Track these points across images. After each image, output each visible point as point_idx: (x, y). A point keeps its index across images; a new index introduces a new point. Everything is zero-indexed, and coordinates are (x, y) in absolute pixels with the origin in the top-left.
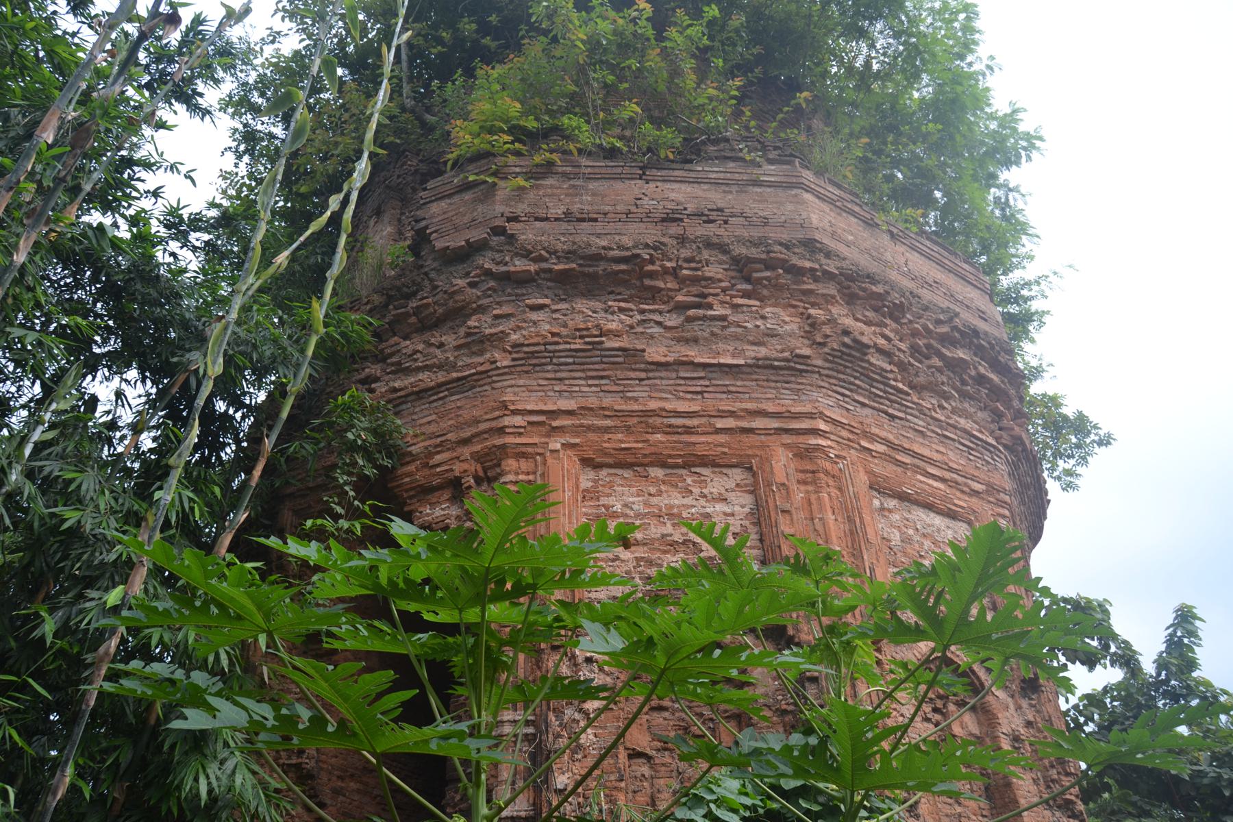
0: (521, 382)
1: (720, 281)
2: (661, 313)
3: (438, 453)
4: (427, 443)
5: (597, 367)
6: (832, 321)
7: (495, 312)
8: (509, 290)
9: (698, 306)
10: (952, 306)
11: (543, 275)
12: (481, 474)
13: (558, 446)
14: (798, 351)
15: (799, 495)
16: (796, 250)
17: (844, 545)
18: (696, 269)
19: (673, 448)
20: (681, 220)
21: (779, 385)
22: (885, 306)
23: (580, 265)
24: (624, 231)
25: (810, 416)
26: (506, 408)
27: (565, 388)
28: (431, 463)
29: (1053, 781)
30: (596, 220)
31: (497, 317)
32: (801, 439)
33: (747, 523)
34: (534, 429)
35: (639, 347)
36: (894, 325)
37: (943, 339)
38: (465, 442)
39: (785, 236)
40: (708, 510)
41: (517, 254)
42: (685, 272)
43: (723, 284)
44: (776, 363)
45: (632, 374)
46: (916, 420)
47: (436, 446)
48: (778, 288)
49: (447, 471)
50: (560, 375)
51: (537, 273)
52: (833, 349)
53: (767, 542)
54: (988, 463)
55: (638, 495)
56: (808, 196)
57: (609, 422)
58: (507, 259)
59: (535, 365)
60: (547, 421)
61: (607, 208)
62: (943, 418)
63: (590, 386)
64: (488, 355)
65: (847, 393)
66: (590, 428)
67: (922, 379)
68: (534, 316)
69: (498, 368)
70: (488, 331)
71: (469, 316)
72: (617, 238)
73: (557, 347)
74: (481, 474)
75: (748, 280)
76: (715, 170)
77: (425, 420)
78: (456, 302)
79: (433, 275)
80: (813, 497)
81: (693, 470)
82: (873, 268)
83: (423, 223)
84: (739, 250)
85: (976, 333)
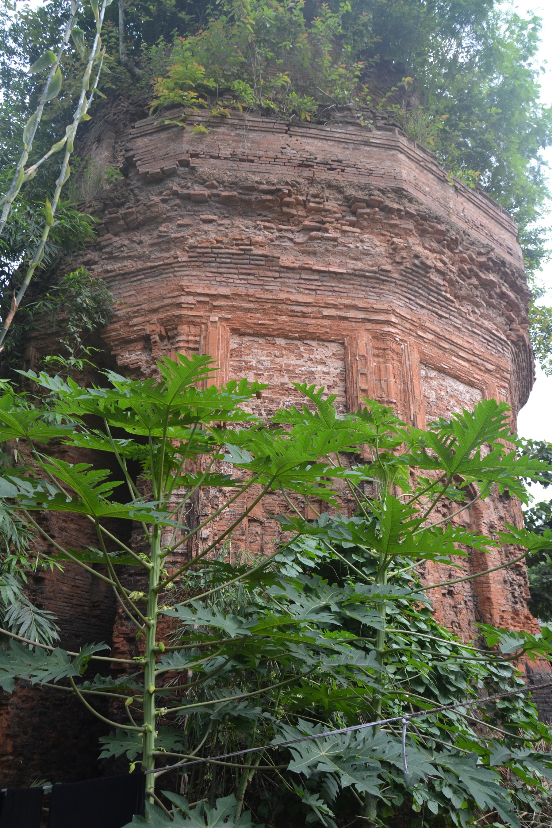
0: (194, 273)
1: (335, 212)
2: (292, 232)
3: (136, 317)
4: (128, 310)
5: (246, 266)
6: (408, 248)
7: (179, 222)
8: (189, 207)
9: (318, 229)
10: (490, 243)
11: (213, 198)
12: (164, 333)
13: (217, 319)
14: (383, 267)
15: (373, 364)
16: (389, 195)
17: (399, 399)
18: (319, 203)
19: (293, 326)
20: (312, 166)
21: (368, 289)
22: (445, 240)
23: (240, 193)
24: (272, 171)
25: (387, 312)
26: (183, 290)
27: (224, 279)
28: (131, 323)
29: (510, 553)
30: (252, 161)
31: (180, 226)
32: (378, 327)
33: (337, 380)
34: (201, 306)
35: (276, 255)
36: (450, 254)
37: (483, 266)
38: (154, 311)
39: (382, 185)
40: (313, 369)
41: (196, 182)
42: (312, 204)
43: (337, 215)
44: (367, 274)
45: (270, 274)
46: (456, 320)
47: (135, 312)
48: (374, 221)
49: (141, 330)
50: (220, 270)
51: (209, 196)
52: (407, 268)
53: (349, 393)
54: (499, 351)
55: (268, 356)
56: (401, 156)
57: (251, 305)
58: (189, 184)
59: (204, 262)
60: (210, 301)
61: (261, 153)
62: (474, 320)
63: (241, 279)
64: (172, 253)
65: (413, 298)
66: (238, 308)
67: (463, 292)
68: (206, 227)
69: (179, 262)
70: (173, 235)
71: (161, 223)
72: (267, 175)
73: (220, 251)
74: (164, 333)
75: (354, 213)
76: (339, 132)
77: (127, 294)
78: (152, 212)
79: (136, 191)
80: (382, 366)
81: (305, 342)
82: (441, 212)
83: (131, 153)
84: (351, 192)
85: (503, 263)
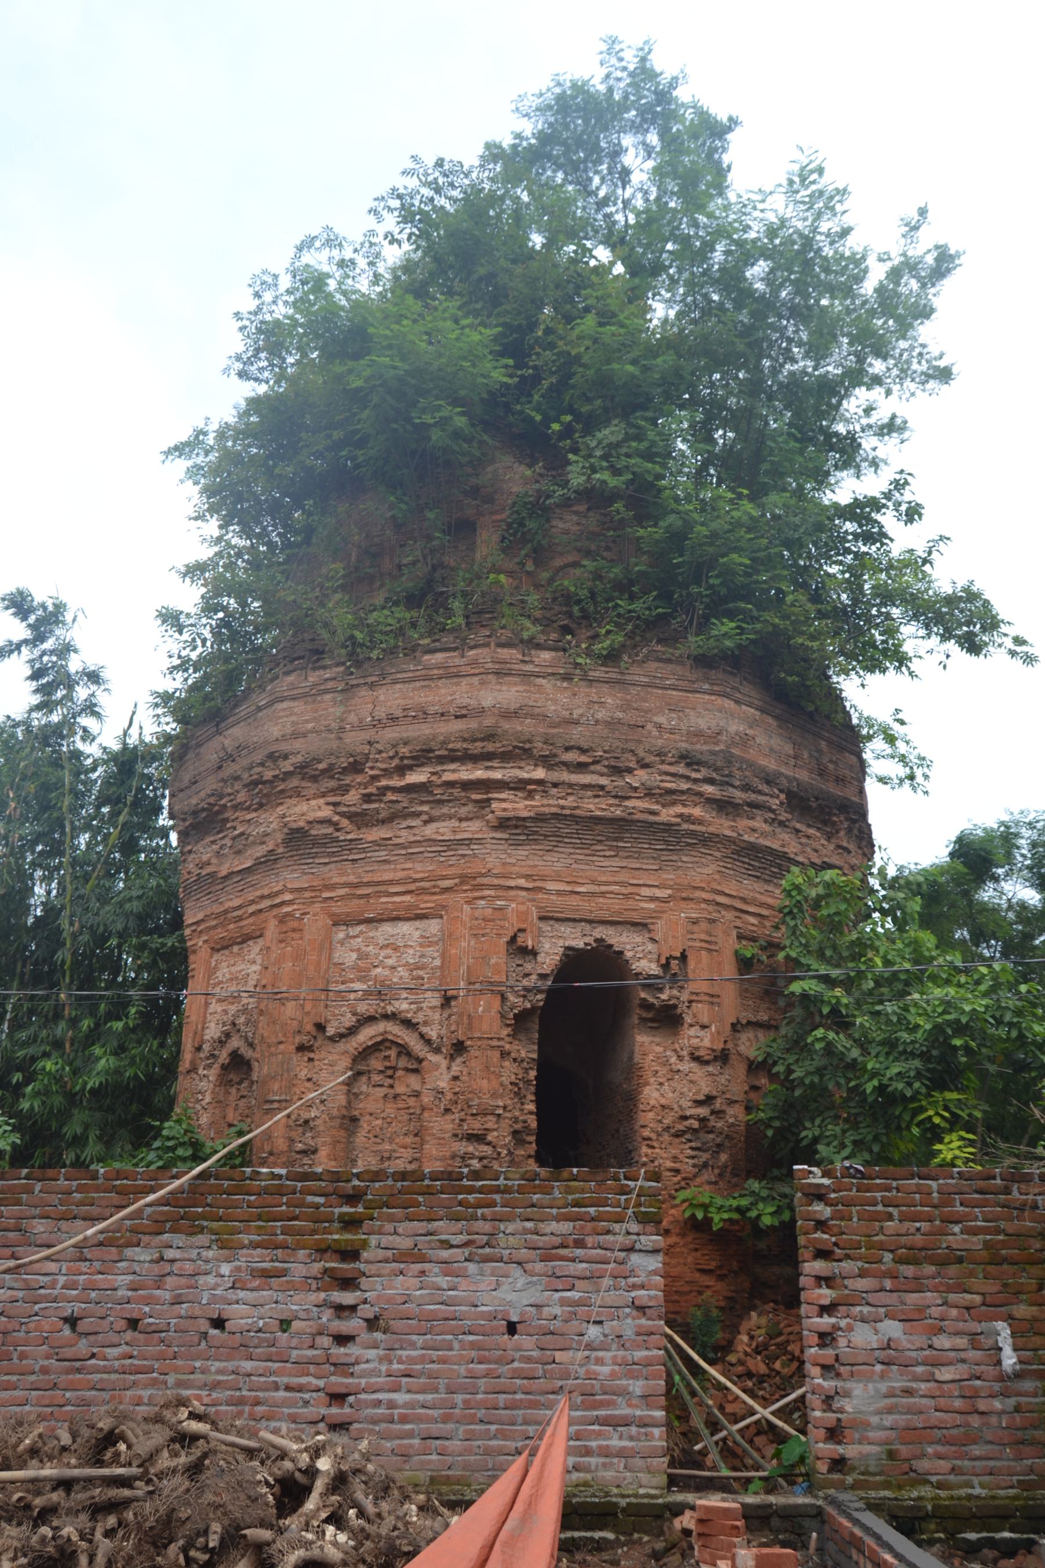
67: (383, 815)
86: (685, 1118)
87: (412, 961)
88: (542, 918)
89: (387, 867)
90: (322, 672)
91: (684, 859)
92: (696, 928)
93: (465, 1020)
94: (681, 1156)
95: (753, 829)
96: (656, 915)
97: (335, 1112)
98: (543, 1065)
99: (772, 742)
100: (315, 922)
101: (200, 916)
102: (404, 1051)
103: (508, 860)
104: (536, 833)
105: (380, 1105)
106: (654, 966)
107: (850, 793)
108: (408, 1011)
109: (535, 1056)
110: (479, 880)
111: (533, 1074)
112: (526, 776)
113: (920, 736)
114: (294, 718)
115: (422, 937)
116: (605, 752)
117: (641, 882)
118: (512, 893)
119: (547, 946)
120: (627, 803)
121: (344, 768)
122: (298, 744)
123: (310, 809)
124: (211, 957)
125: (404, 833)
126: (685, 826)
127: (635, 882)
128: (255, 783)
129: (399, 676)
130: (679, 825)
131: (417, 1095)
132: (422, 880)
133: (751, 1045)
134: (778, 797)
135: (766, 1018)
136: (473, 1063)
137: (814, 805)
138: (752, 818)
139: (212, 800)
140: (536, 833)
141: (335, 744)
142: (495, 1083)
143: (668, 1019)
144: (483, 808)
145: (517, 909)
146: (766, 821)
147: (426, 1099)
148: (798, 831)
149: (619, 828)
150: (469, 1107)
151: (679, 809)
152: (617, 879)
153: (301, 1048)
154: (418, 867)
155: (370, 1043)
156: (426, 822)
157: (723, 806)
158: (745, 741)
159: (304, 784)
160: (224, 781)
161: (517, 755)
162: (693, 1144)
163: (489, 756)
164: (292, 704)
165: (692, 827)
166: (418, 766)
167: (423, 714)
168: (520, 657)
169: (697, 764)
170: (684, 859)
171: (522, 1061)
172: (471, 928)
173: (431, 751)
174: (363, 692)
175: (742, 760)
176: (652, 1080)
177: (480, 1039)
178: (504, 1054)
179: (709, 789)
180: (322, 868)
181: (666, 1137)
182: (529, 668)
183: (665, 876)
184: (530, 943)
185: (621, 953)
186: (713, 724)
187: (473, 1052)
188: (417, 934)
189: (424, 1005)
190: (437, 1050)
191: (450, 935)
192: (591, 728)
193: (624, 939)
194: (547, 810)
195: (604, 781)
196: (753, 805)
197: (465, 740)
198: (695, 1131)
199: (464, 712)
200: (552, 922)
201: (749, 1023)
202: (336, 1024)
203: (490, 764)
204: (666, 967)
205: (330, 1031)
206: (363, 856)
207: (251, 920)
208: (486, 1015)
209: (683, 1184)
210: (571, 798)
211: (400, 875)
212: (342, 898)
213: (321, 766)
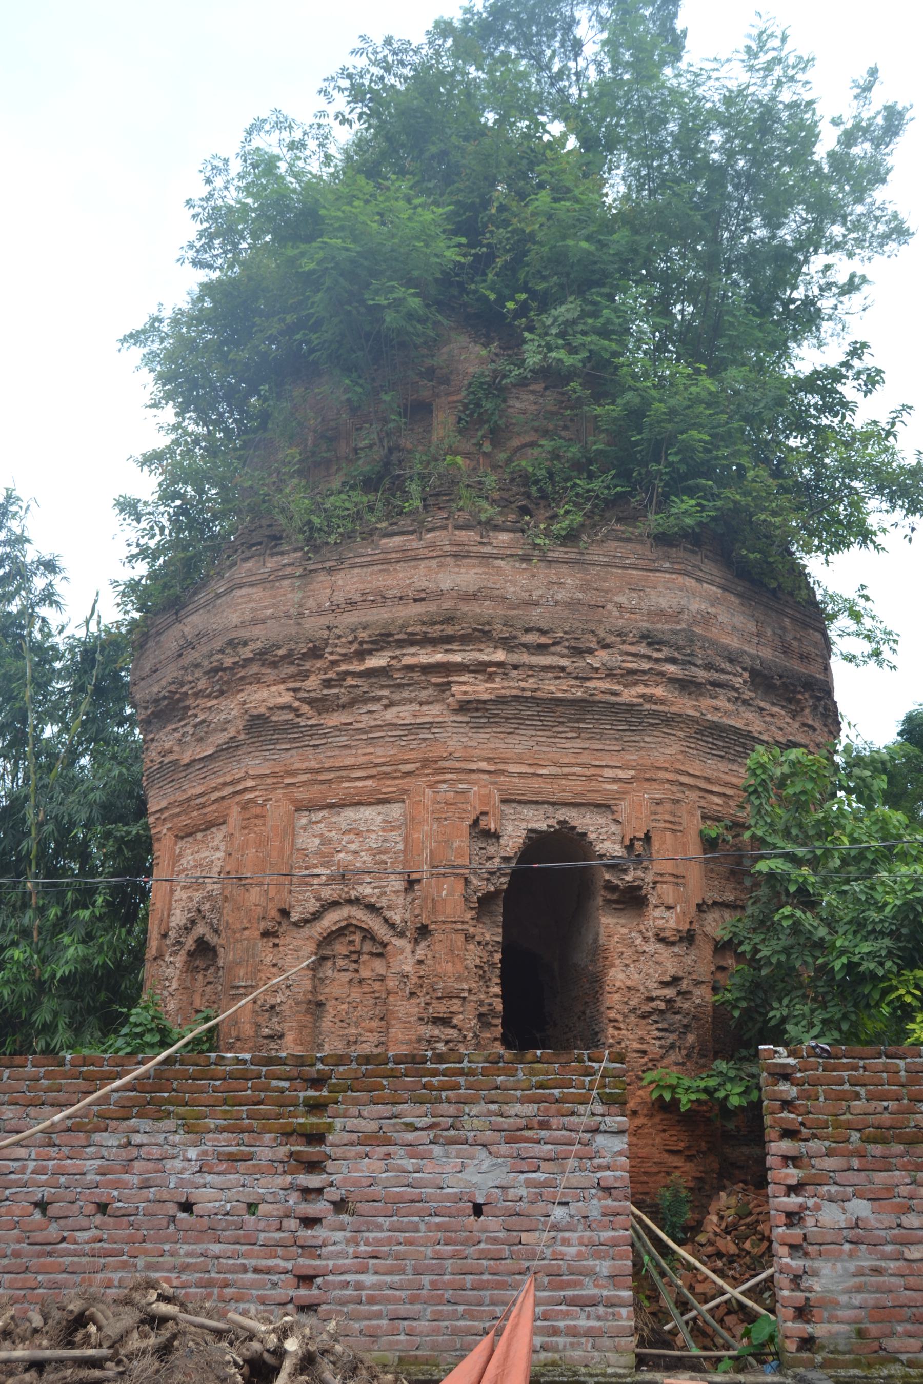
46: (338, 739)
67: (344, 700)
86: (651, 999)
87: (374, 846)
88: (504, 801)
89: (348, 752)
90: (279, 558)
91: (647, 739)
92: (659, 809)
93: (429, 905)
94: (647, 1038)
95: (716, 708)
96: (619, 796)
97: (301, 997)
98: (508, 948)
99: (735, 620)
100: (277, 808)
101: (164, 804)
102: (368, 935)
103: (470, 744)
104: (497, 715)
105: (346, 990)
106: (617, 847)
107: (814, 670)
108: (371, 896)
109: (499, 939)
110: (442, 764)
111: (498, 957)
112: (486, 658)
113: (885, 611)
114: (253, 605)
115: (385, 821)
116: (565, 633)
117: (604, 763)
118: (474, 776)
119: (510, 829)
120: (588, 684)
121: (303, 654)
122: (258, 631)
123: (270, 695)
124: (176, 844)
125: (365, 718)
126: (647, 706)
127: (597, 763)
128: (216, 670)
129: (357, 560)
130: (641, 705)
131: (382, 979)
132: (383, 764)
133: (716, 926)
134: (741, 675)
135: (732, 898)
136: (438, 947)
137: (778, 683)
138: (716, 697)
139: (173, 688)
140: (497, 715)
141: (293, 631)
142: (459, 967)
143: (632, 900)
144: (443, 691)
145: (479, 793)
146: (729, 700)
147: (391, 983)
148: (762, 709)
149: (581, 710)
150: (434, 990)
151: (641, 689)
152: (579, 761)
153: (266, 934)
154: (380, 751)
155: (334, 929)
156: (386, 707)
157: (685, 685)
158: (707, 619)
159: (264, 670)
160: (184, 668)
161: (477, 637)
162: (660, 1026)
163: (448, 639)
164: (250, 590)
165: (654, 707)
166: (377, 650)
167: (381, 598)
168: (478, 539)
169: (658, 643)
170: (647, 739)
171: (487, 944)
172: (433, 812)
173: (390, 635)
174: (322, 577)
175: (704, 639)
176: (617, 962)
177: (444, 922)
178: (468, 938)
179: (671, 669)
180: (285, 755)
181: (632, 1018)
182: (487, 549)
183: (628, 757)
184: (492, 826)
185: (585, 834)
186: (674, 603)
187: (438, 936)
188: (380, 818)
189: (388, 890)
190: (402, 935)
191: (413, 819)
192: (551, 609)
193: (587, 820)
194: (507, 692)
195: (564, 662)
196: (715, 684)
197: (424, 623)
198: (662, 1012)
199: (423, 595)
200: (514, 805)
201: (715, 903)
202: (300, 909)
203: (450, 647)
204: (630, 848)
205: (295, 917)
206: (324, 741)
207: (214, 807)
208: (450, 898)
209: (650, 1065)
210: (531, 680)
211: (361, 760)
212: (304, 783)
213: (281, 652)
